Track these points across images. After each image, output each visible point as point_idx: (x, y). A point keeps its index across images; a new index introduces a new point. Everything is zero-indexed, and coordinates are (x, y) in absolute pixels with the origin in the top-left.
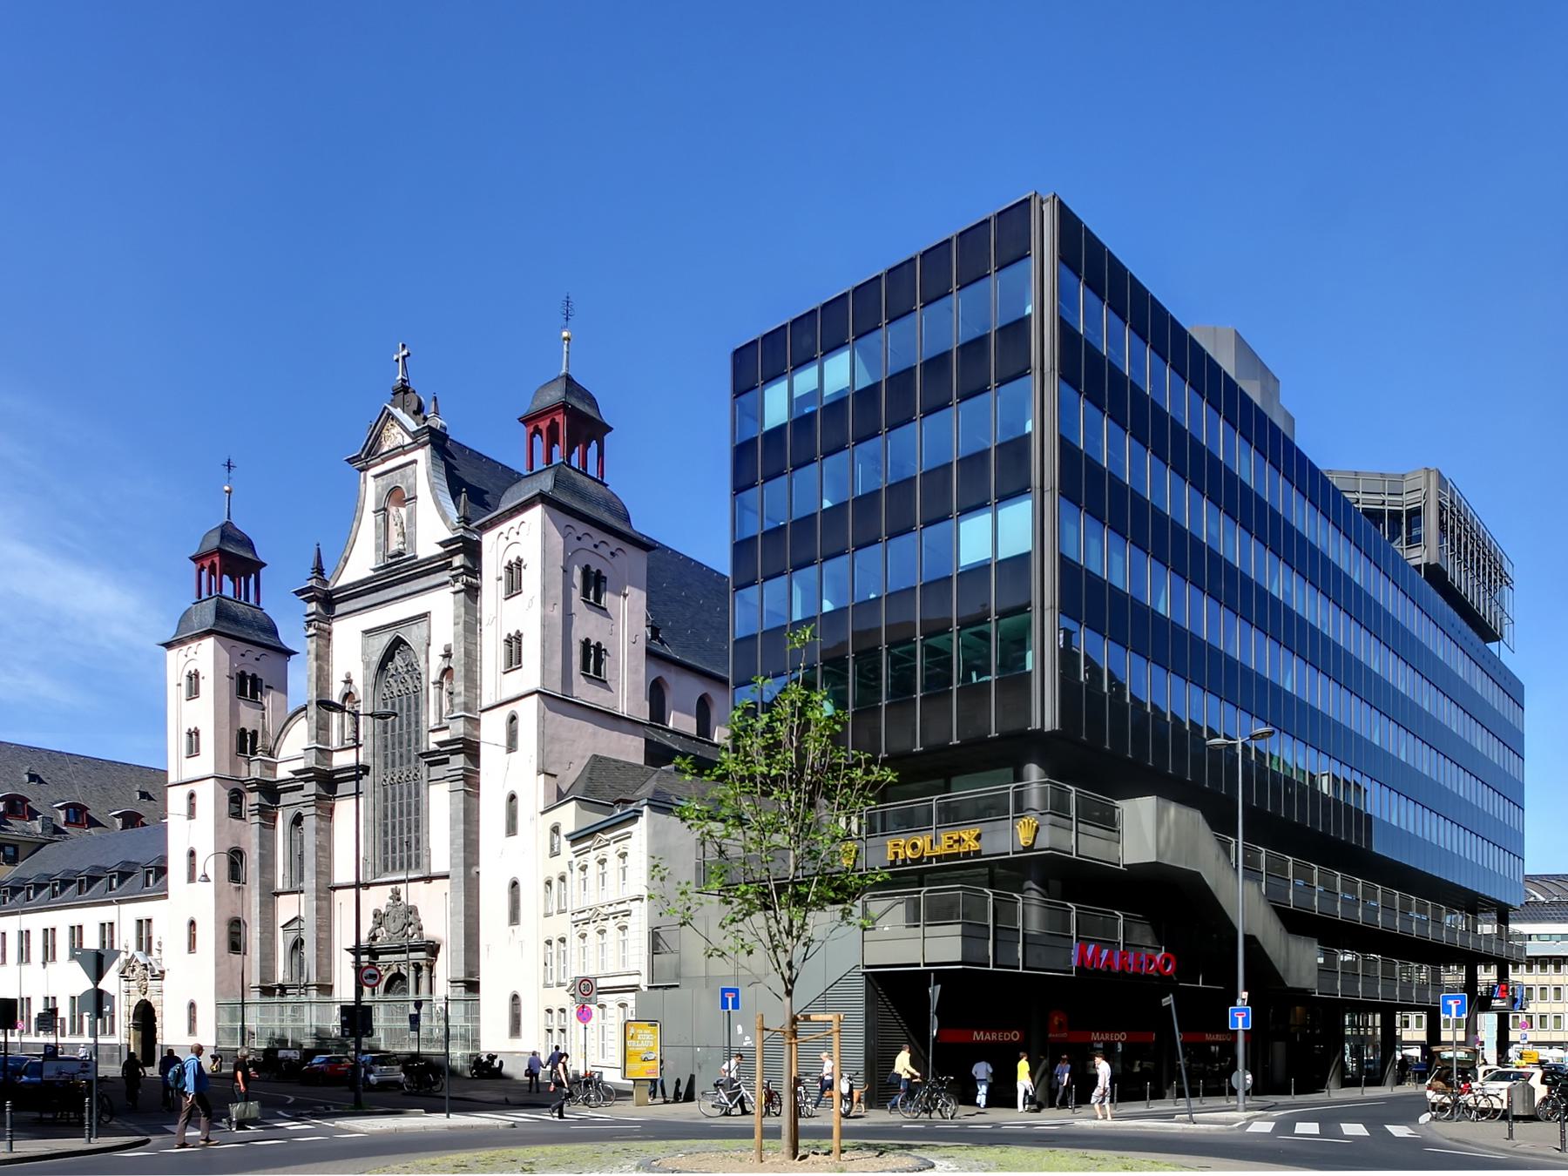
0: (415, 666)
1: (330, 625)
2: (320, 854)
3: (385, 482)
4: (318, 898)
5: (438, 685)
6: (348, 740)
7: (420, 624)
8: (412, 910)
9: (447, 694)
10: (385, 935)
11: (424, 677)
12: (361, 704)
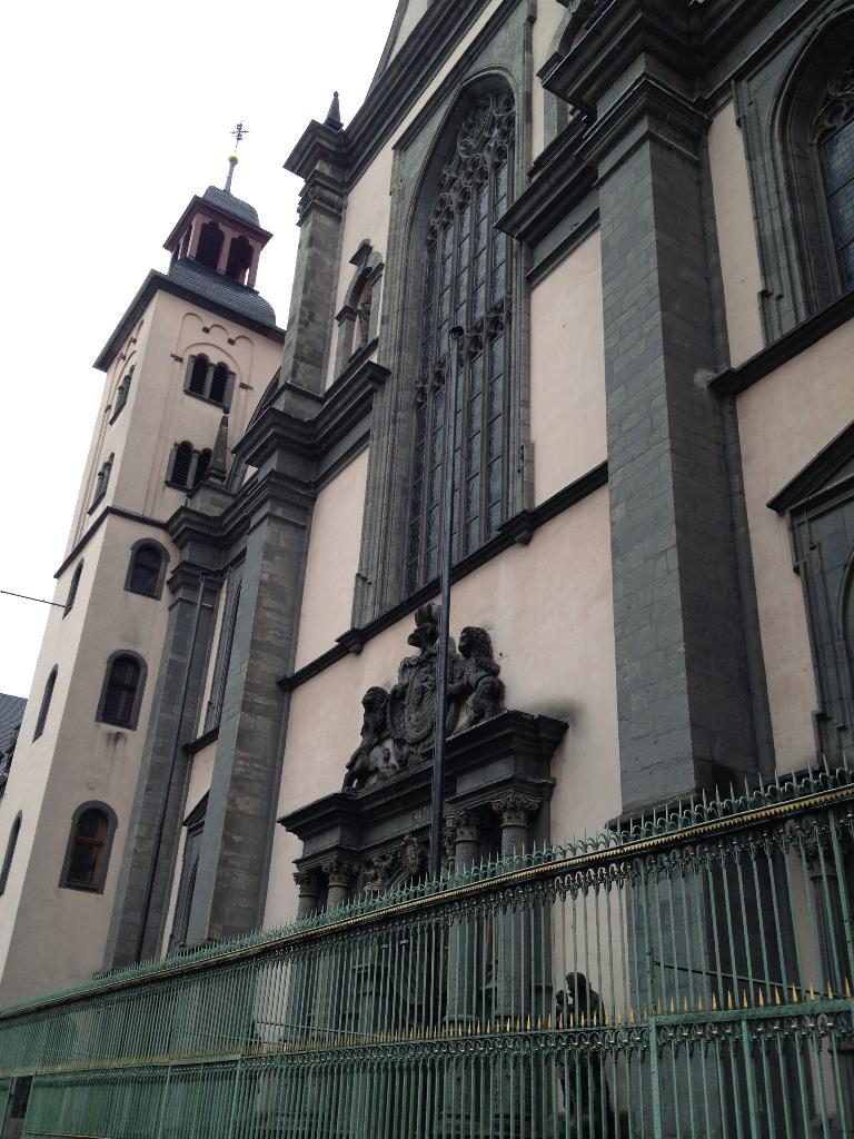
1: (344, 195)
2: (267, 602)
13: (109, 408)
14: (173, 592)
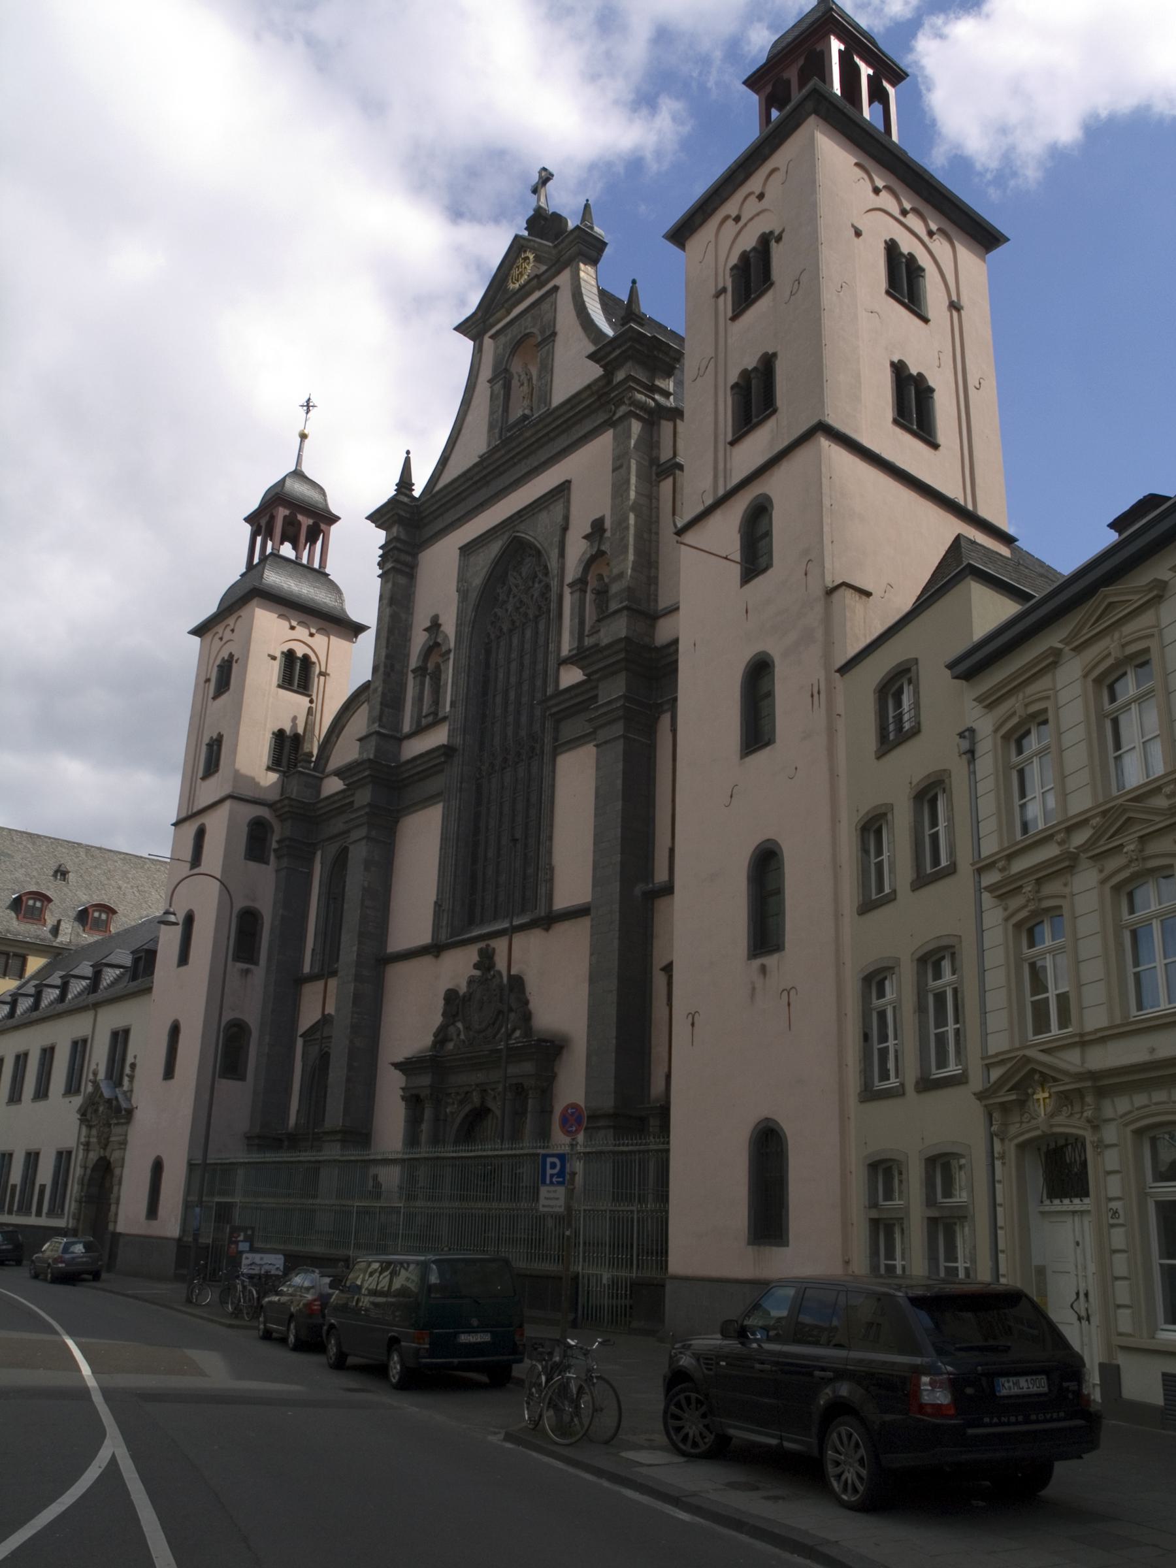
0: (540, 575)
1: (415, 556)
3: (509, 336)
4: (358, 978)
5: (579, 586)
6: (426, 716)
7: (551, 507)
8: (517, 983)
9: (594, 596)
10: (462, 1037)
11: (554, 584)
12: (452, 656)
13: (208, 680)
14: (278, 858)
